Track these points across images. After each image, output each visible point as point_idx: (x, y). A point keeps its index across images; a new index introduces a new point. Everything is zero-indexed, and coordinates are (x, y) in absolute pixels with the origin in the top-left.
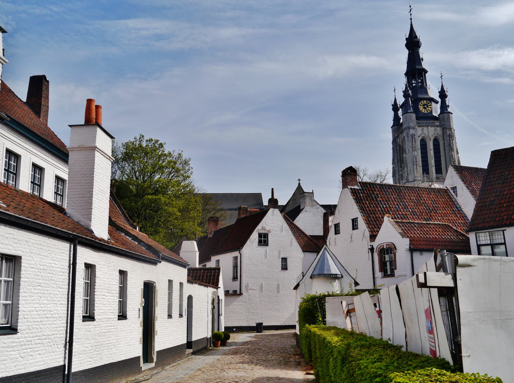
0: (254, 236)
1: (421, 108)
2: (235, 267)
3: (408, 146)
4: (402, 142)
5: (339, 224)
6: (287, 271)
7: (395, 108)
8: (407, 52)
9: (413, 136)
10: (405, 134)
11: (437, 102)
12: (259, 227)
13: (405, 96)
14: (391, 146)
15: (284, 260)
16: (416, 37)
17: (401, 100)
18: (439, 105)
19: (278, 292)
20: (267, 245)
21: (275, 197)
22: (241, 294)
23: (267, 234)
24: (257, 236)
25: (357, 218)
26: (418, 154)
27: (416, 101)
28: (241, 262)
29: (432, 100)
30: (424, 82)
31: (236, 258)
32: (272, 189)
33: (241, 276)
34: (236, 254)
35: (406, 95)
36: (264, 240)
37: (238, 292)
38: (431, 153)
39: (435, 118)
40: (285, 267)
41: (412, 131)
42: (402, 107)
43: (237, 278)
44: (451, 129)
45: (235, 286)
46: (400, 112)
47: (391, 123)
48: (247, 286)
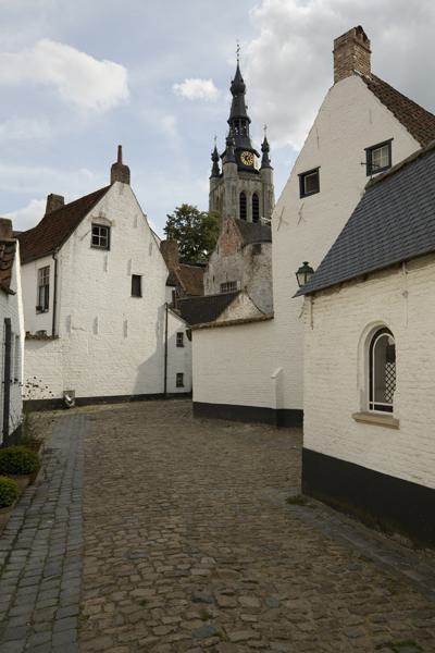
0: (85, 228)
1: (243, 160)
2: (44, 287)
3: (227, 198)
4: (222, 195)
5: (316, 170)
6: (140, 300)
7: (215, 158)
8: (230, 97)
9: (234, 188)
10: (225, 185)
11: (258, 156)
12: (94, 212)
13: (227, 144)
14: (208, 199)
15: (137, 280)
16: (242, 81)
17: (222, 149)
18: (260, 159)
19: (126, 335)
20: (108, 249)
21: (125, 162)
22: (54, 337)
23: (109, 228)
24: (90, 228)
25: (388, 144)
26: (237, 207)
27: (239, 151)
28: (56, 276)
29: (254, 152)
30: (246, 132)
31: (45, 271)
32: (120, 147)
33: (55, 302)
34: (48, 261)
35: (229, 143)
36: (101, 237)
37: (49, 334)
38: (250, 208)
39: (256, 172)
40: (137, 291)
41: (233, 183)
42: (222, 157)
43: (47, 306)
44: (271, 185)
45: (44, 322)
46: (220, 163)
47: (210, 174)
48: (68, 323)
